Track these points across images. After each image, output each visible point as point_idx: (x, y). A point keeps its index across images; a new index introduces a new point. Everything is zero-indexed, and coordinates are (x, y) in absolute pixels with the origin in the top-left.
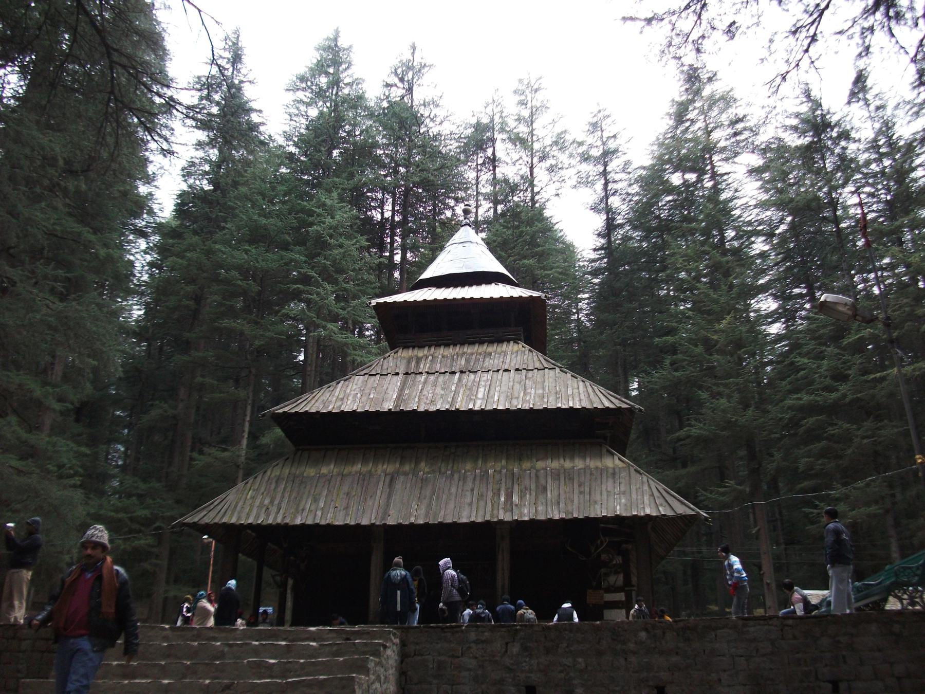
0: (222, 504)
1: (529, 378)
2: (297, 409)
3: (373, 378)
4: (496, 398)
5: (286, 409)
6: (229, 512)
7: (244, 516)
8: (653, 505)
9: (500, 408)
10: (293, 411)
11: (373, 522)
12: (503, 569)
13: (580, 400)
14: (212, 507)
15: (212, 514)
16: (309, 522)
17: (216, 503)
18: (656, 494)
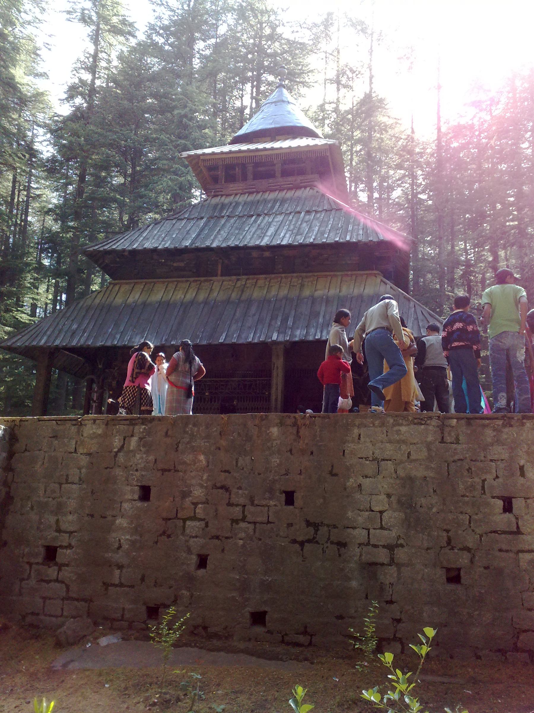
0: (37, 329)
1: (317, 219)
2: (106, 247)
3: (180, 222)
4: (282, 235)
5: (96, 248)
6: (39, 338)
7: (52, 340)
8: (416, 327)
9: (284, 243)
10: (101, 249)
11: (163, 343)
12: (277, 385)
13: (358, 235)
14: (26, 332)
15: (25, 338)
16: (109, 344)
17: (29, 330)
18: (420, 317)
